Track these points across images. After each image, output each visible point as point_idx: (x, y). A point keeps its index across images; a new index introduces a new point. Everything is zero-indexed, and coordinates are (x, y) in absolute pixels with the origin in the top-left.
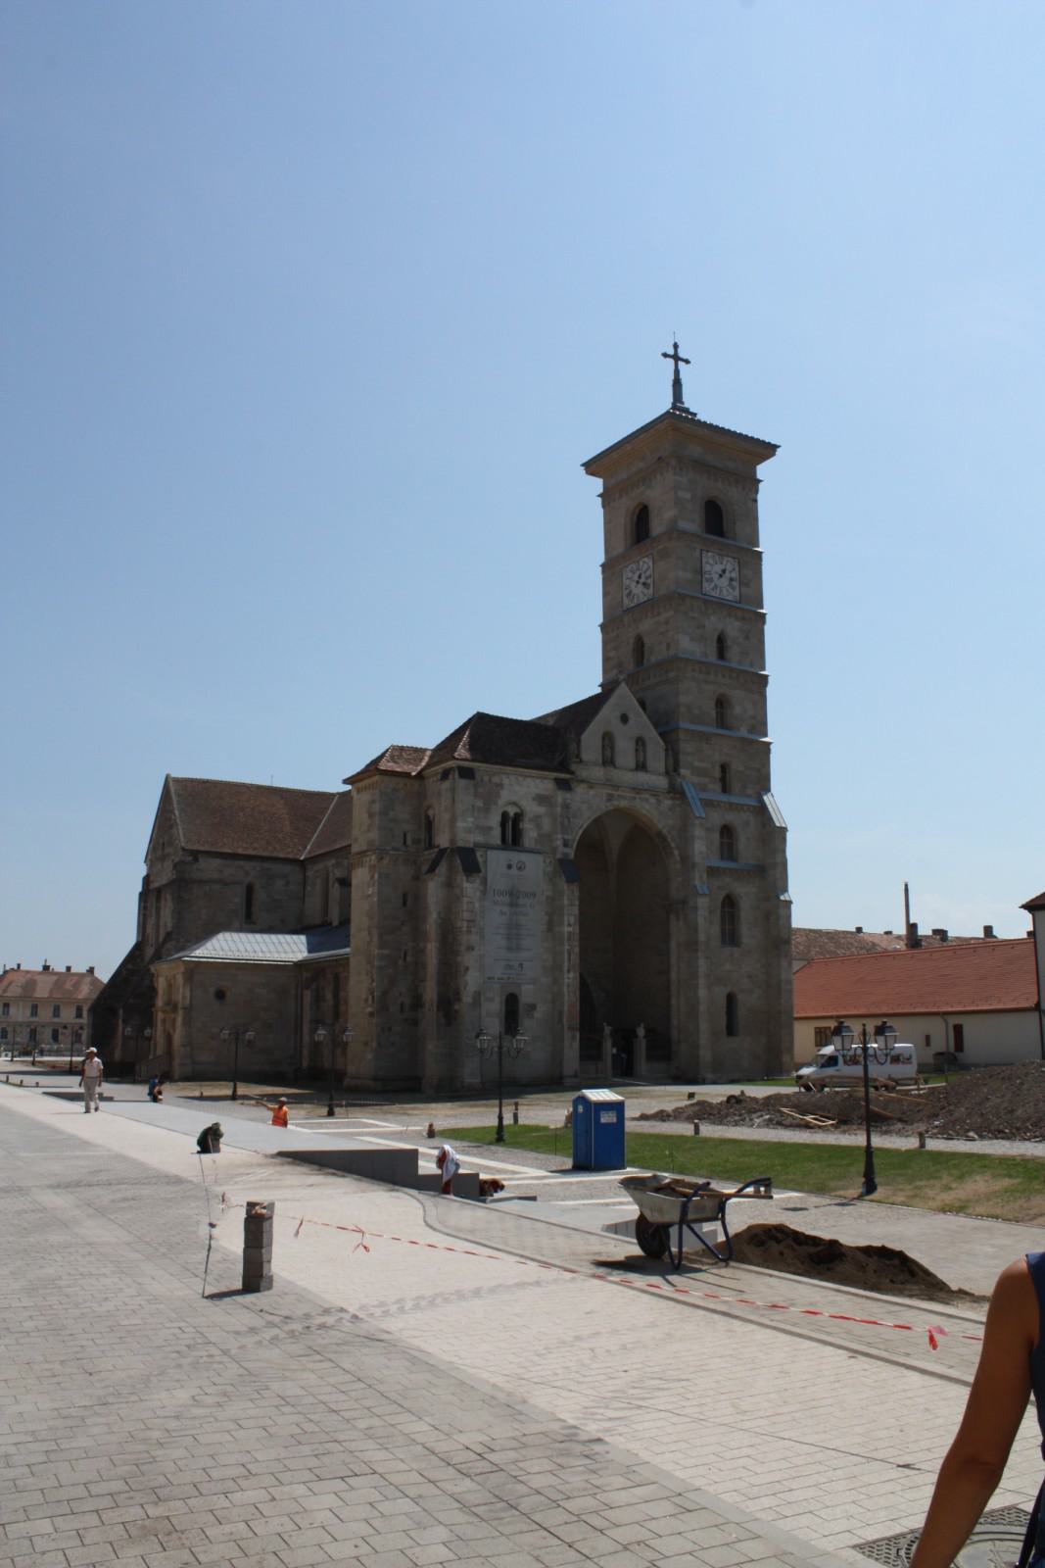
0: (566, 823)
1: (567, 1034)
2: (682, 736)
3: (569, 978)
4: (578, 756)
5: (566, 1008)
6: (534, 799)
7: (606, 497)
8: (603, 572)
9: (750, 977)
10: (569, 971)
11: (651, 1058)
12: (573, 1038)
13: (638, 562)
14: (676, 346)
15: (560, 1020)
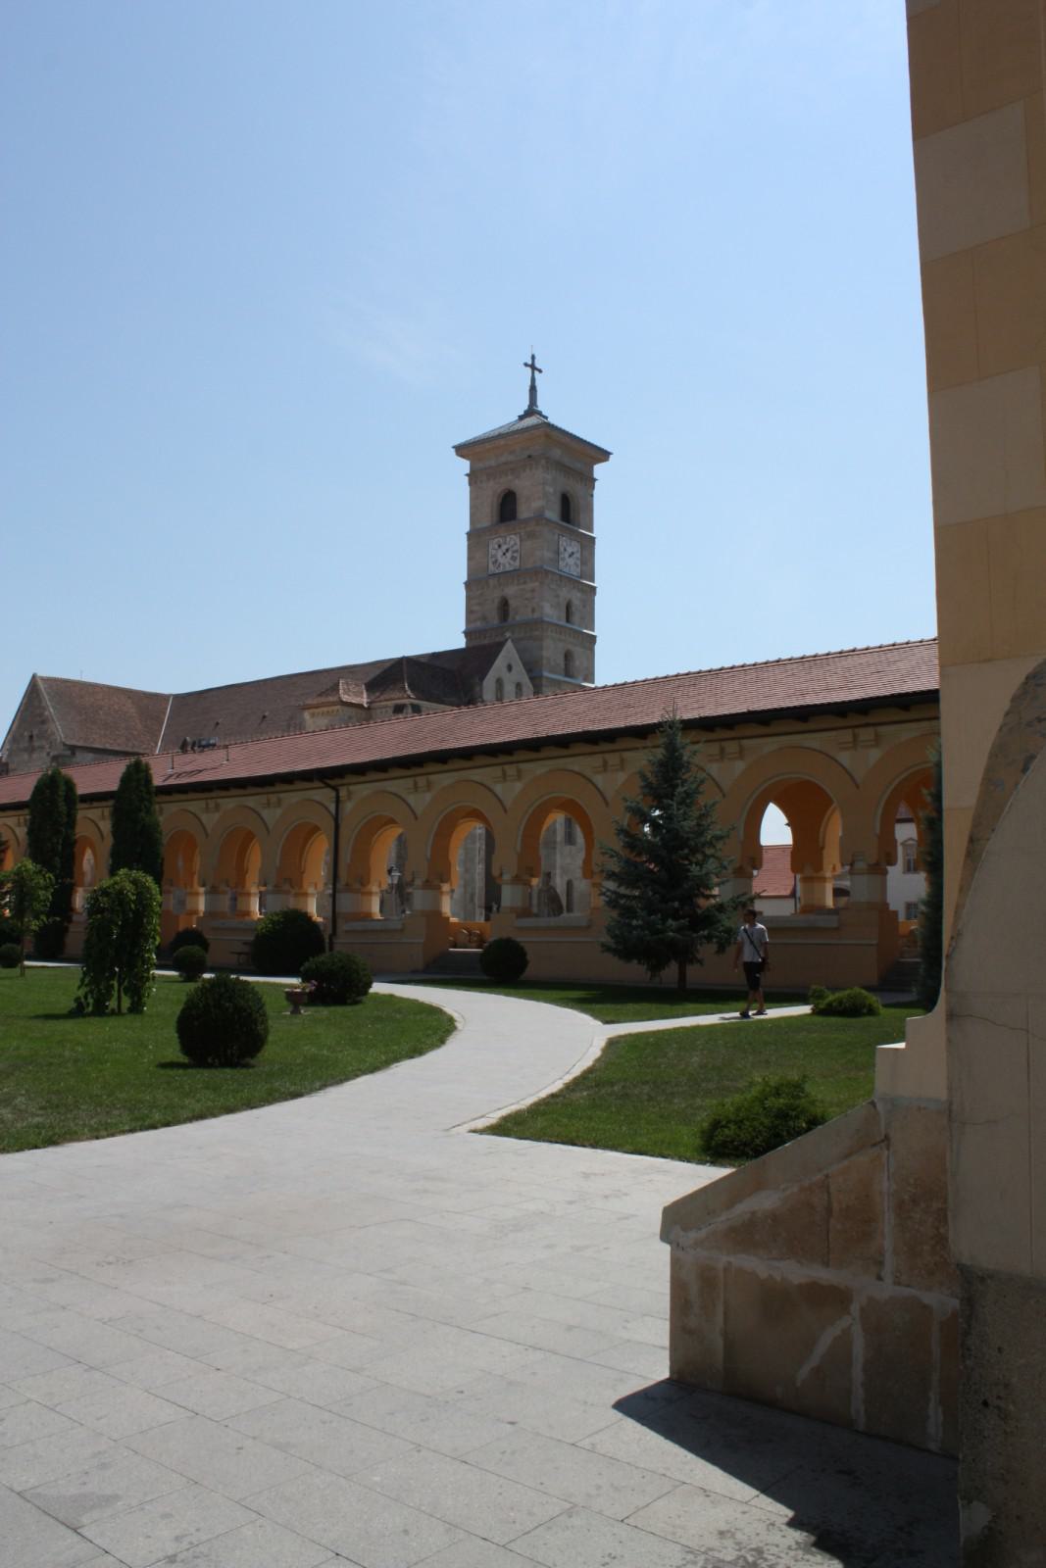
1: (478, 911)
2: (544, 682)
4: (481, 697)
7: (473, 477)
8: (469, 539)
12: (481, 914)
13: (505, 537)
14: (533, 357)
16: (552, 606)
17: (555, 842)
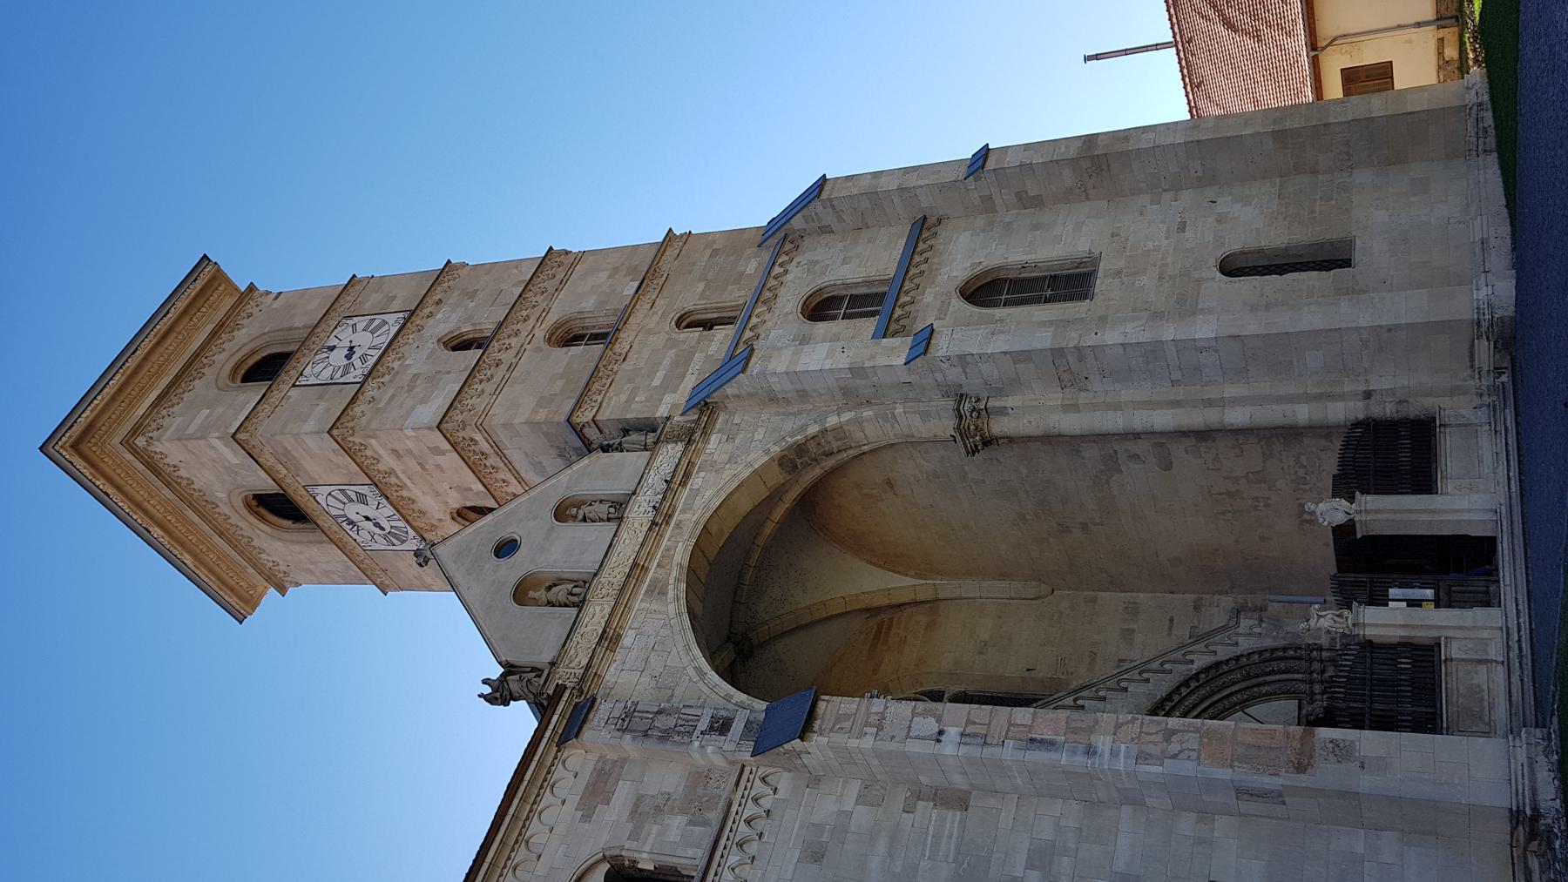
3: (1114, 754)
5: (1223, 774)
6: (587, 817)
9: (1182, 227)
11: (1423, 481)
12: (1341, 752)
15: (1275, 797)
16: (424, 401)
17: (1057, 353)
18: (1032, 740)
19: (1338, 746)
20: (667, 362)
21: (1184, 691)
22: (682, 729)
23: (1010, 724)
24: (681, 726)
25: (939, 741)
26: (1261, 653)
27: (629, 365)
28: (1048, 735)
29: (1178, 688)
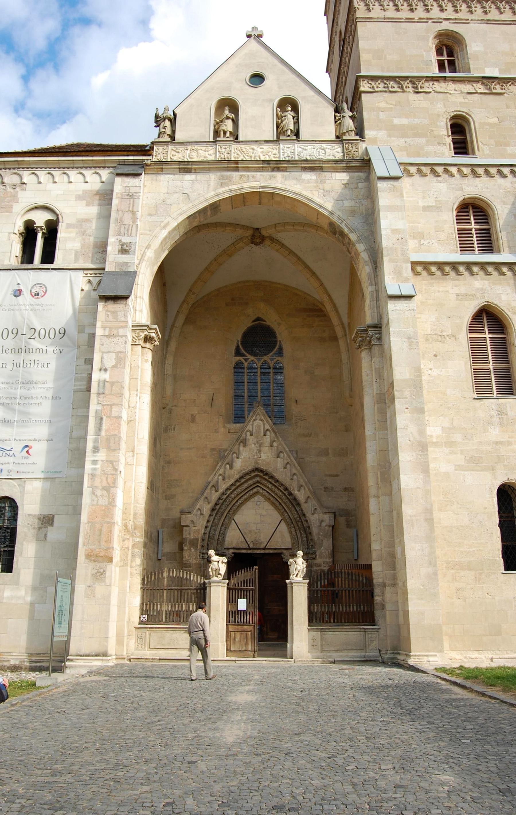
0: (127, 219)
6: (79, 198)
10: (96, 449)
18: (102, 419)
19: (102, 574)
20: (417, 121)
21: (282, 488)
22: (122, 229)
23: (111, 406)
24: (125, 228)
25: (100, 370)
26: (309, 527)
27: (412, 97)
28: (104, 427)
29: (282, 485)
